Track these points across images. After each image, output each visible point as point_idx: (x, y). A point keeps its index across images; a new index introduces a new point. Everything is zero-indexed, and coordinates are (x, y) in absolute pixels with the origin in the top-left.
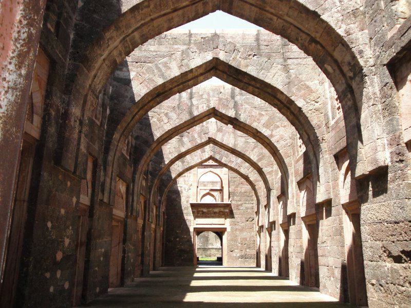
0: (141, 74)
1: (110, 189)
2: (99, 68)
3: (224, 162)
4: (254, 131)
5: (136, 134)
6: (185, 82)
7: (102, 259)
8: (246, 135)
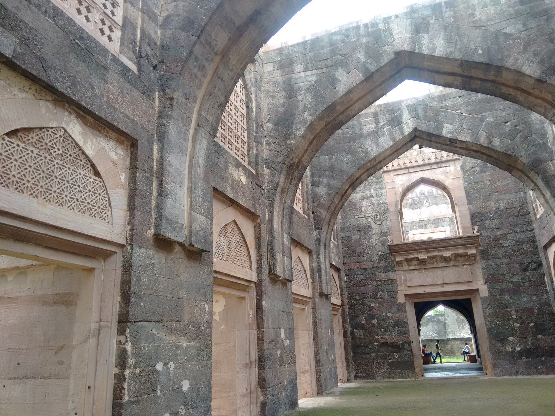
3: (449, 136)
5: (165, 14)
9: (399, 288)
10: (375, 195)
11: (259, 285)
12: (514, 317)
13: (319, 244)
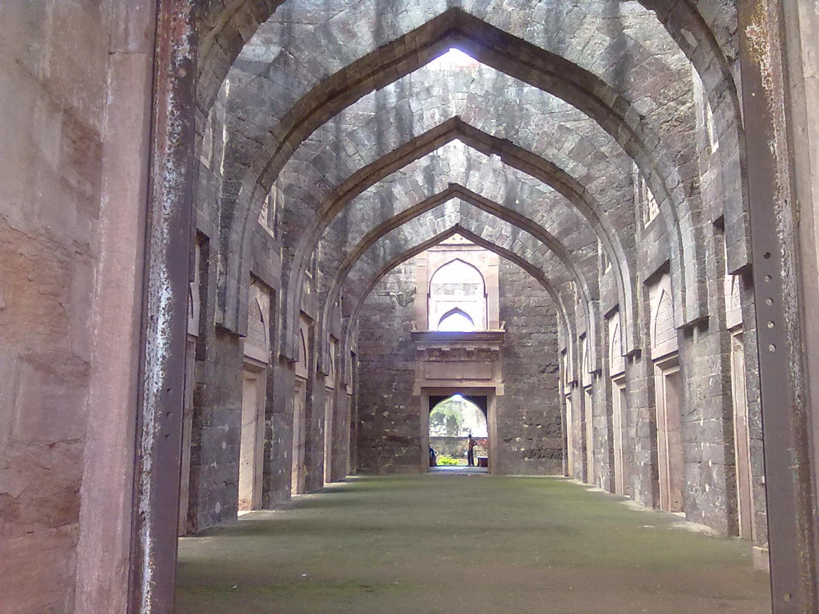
0: (292, 50)
1: (238, 300)
2: (208, 54)
4: (548, 168)
5: (288, 181)
6: (388, 65)
7: (224, 445)
8: (532, 177)
9: (416, 380)
10: (403, 271)
11: (309, 381)
12: (524, 418)
13: (345, 333)
